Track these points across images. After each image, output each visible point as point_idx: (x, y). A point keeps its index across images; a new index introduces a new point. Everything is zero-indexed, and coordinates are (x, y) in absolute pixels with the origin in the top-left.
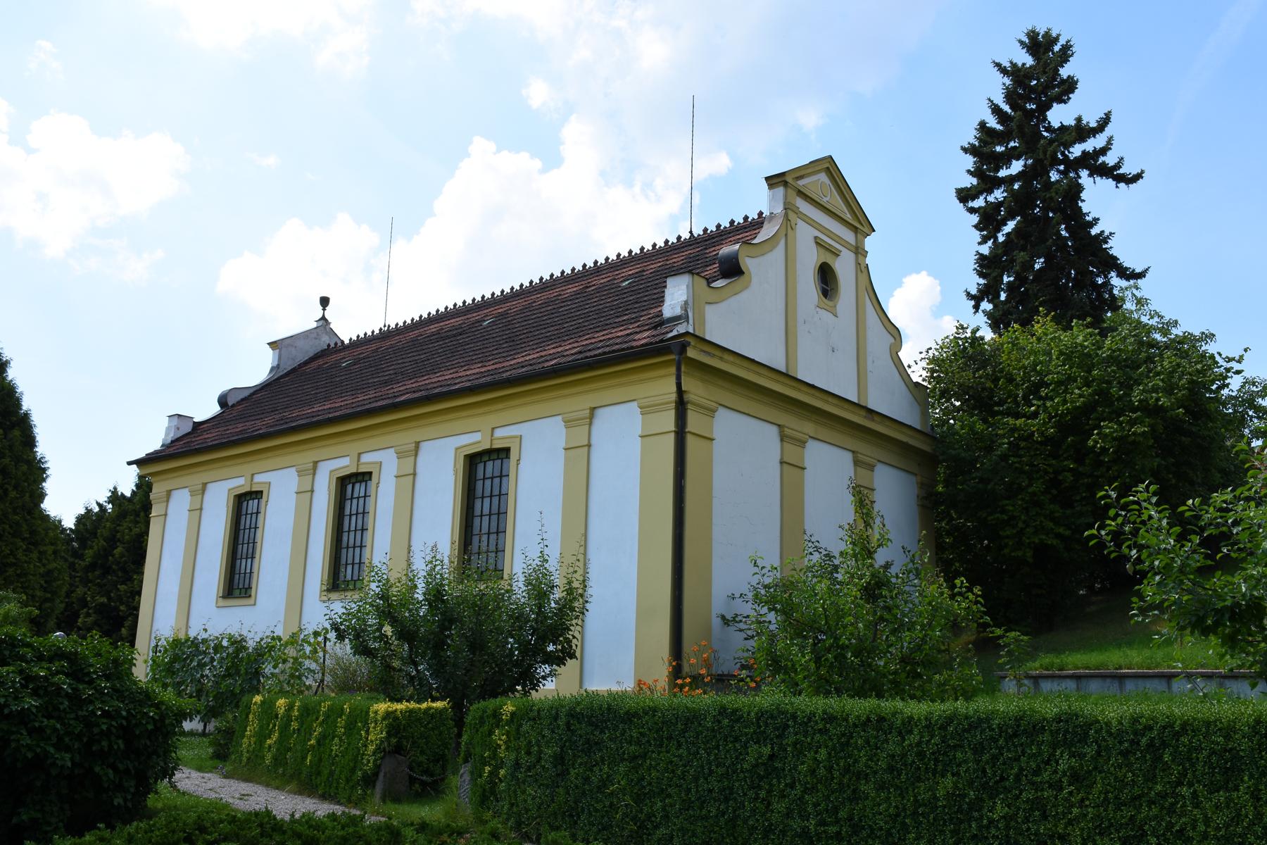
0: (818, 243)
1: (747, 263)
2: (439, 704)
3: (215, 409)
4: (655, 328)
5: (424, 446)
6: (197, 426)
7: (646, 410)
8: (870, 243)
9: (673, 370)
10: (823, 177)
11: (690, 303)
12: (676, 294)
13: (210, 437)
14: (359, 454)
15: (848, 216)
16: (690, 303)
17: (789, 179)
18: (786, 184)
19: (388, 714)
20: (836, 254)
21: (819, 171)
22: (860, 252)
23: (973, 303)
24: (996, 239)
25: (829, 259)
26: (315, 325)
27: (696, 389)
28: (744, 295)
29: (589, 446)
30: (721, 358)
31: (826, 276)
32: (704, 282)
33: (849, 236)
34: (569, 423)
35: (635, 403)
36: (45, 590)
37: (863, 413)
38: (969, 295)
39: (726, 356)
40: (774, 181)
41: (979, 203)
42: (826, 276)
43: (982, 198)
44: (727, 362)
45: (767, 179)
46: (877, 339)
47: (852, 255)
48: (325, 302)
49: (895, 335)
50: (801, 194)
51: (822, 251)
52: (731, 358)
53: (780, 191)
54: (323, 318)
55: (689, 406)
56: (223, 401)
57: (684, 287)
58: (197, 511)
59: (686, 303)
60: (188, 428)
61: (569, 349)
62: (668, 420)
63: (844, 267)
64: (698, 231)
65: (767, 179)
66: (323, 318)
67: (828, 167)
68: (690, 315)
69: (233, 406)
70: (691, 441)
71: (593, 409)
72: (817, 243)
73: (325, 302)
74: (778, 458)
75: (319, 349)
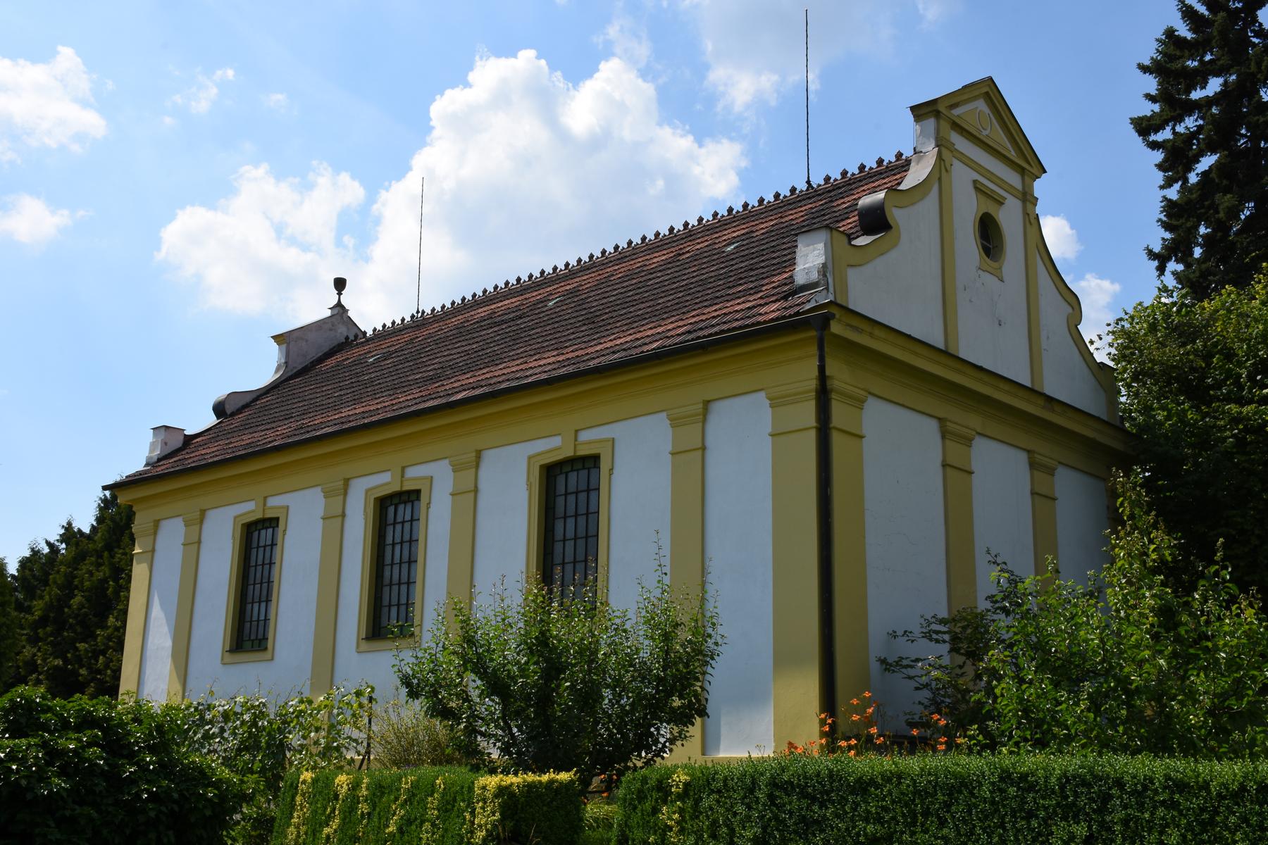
0: (978, 187)
1: (896, 215)
2: (564, 776)
3: (211, 420)
4: (785, 298)
5: (489, 456)
6: (189, 439)
7: (776, 402)
8: (1040, 187)
9: (814, 350)
10: (981, 105)
11: (830, 265)
12: (810, 257)
13: (210, 453)
14: (403, 469)
15: (1012, 154)
16: (830, 265)
17: (942, 108)
18: (937, 114)
19: (502, 791)
21: (975, 98)
22: (1028, 199)
23: (1156, 263)
24: (1186, 180)
26: (328, 313)
28: (893, 254)
29: (704, 448)
30: (871, 335)
31: (989, 233)
32: (845, 239)
33: (1014, 179)
34: (675, 422)
35: (763, 394)
37: (1041, 402)
38: (1151, 255)
39: (877, 332)
40: (920, 112)
41: (1165, 135)
42: (989, 233)
43: (1168, 129)
45: (913, 109)
47: (1018, 203)
48: (340, 284)
49: (1073, 302)
50: (957, 127)
51: (983, 199)
53: (931, 123)
54: (339, 305)
55: (833, 396)
56: (219, 409)
57: (821, 246)
58: (194, 545)
59: (824, 265)
60: (179, 442)
61: (673, 330)
62: (807, 413)
63: (1009, 218)
64: (817, 180)
65: (913, 109)
66: (339, 305)
67: (987, 91)
69: (233, 414)
70: (837, 440)
71: (707, 403)
72: (976, 188)
73: (340, 284)
75: (336, 343)
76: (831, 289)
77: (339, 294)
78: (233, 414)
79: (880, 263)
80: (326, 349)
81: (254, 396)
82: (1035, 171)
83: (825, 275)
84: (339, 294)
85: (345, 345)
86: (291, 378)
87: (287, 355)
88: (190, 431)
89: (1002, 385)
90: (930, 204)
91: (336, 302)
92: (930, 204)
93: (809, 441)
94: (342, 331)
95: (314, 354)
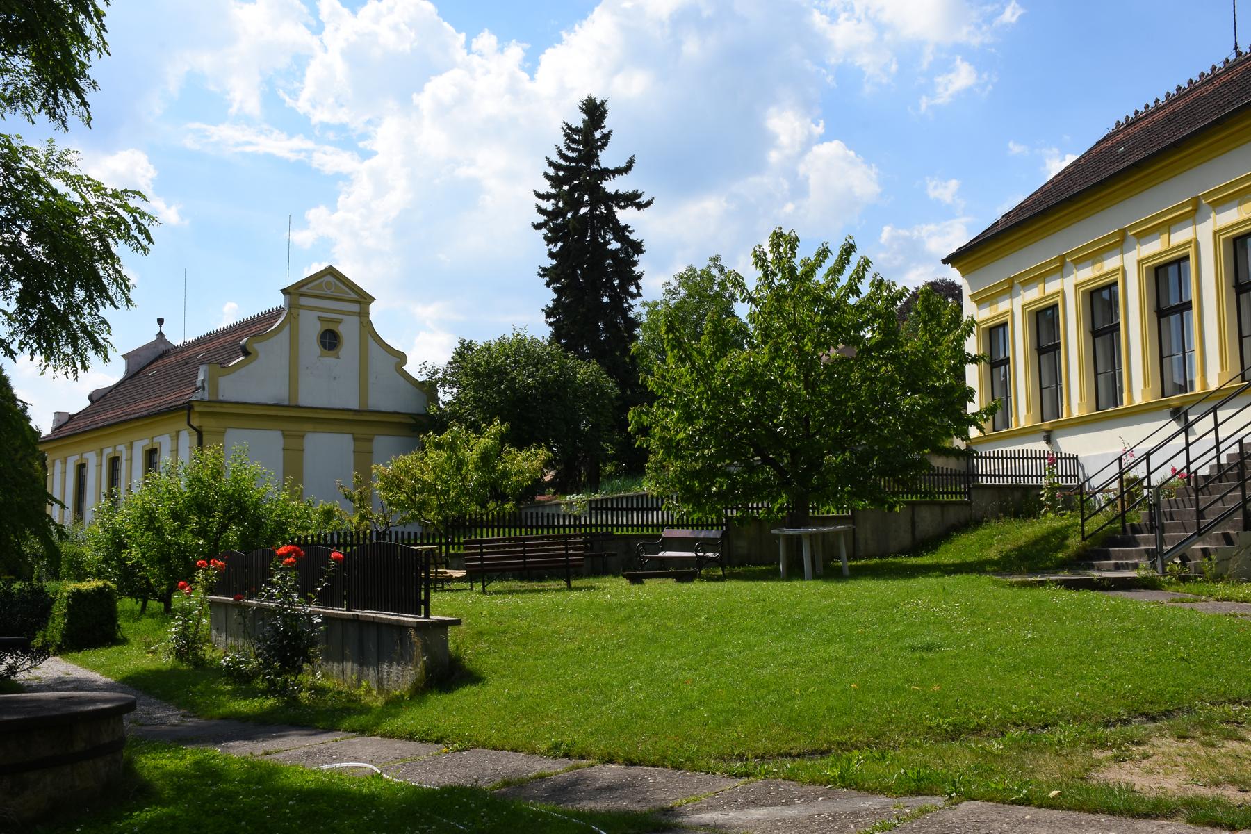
0: (321, 319)
1: (258, 347)
3: (89, 403)
6: (71, 417)
8: (372, 307)
10: (329, 278)
15: (354, 296)
17: (291, 291)
20: (340, 322)
22: (364, 314)
25: (332, 327)
27: (208, 424)
33: (355, 308)
40: (285, 291)
47: (356, 319)
48: (161, 321)
50: (302, 295)
56: (90, 398)
58: (64, 473)
59: (203, 381)
60: (66, 419)
67: (331, 271)
73: (161, 321)
79: (243, 371)
85: (163, 355)
86: (130, 378)
87: (128, 365)
88: (72, 412)
94: (162, 347)
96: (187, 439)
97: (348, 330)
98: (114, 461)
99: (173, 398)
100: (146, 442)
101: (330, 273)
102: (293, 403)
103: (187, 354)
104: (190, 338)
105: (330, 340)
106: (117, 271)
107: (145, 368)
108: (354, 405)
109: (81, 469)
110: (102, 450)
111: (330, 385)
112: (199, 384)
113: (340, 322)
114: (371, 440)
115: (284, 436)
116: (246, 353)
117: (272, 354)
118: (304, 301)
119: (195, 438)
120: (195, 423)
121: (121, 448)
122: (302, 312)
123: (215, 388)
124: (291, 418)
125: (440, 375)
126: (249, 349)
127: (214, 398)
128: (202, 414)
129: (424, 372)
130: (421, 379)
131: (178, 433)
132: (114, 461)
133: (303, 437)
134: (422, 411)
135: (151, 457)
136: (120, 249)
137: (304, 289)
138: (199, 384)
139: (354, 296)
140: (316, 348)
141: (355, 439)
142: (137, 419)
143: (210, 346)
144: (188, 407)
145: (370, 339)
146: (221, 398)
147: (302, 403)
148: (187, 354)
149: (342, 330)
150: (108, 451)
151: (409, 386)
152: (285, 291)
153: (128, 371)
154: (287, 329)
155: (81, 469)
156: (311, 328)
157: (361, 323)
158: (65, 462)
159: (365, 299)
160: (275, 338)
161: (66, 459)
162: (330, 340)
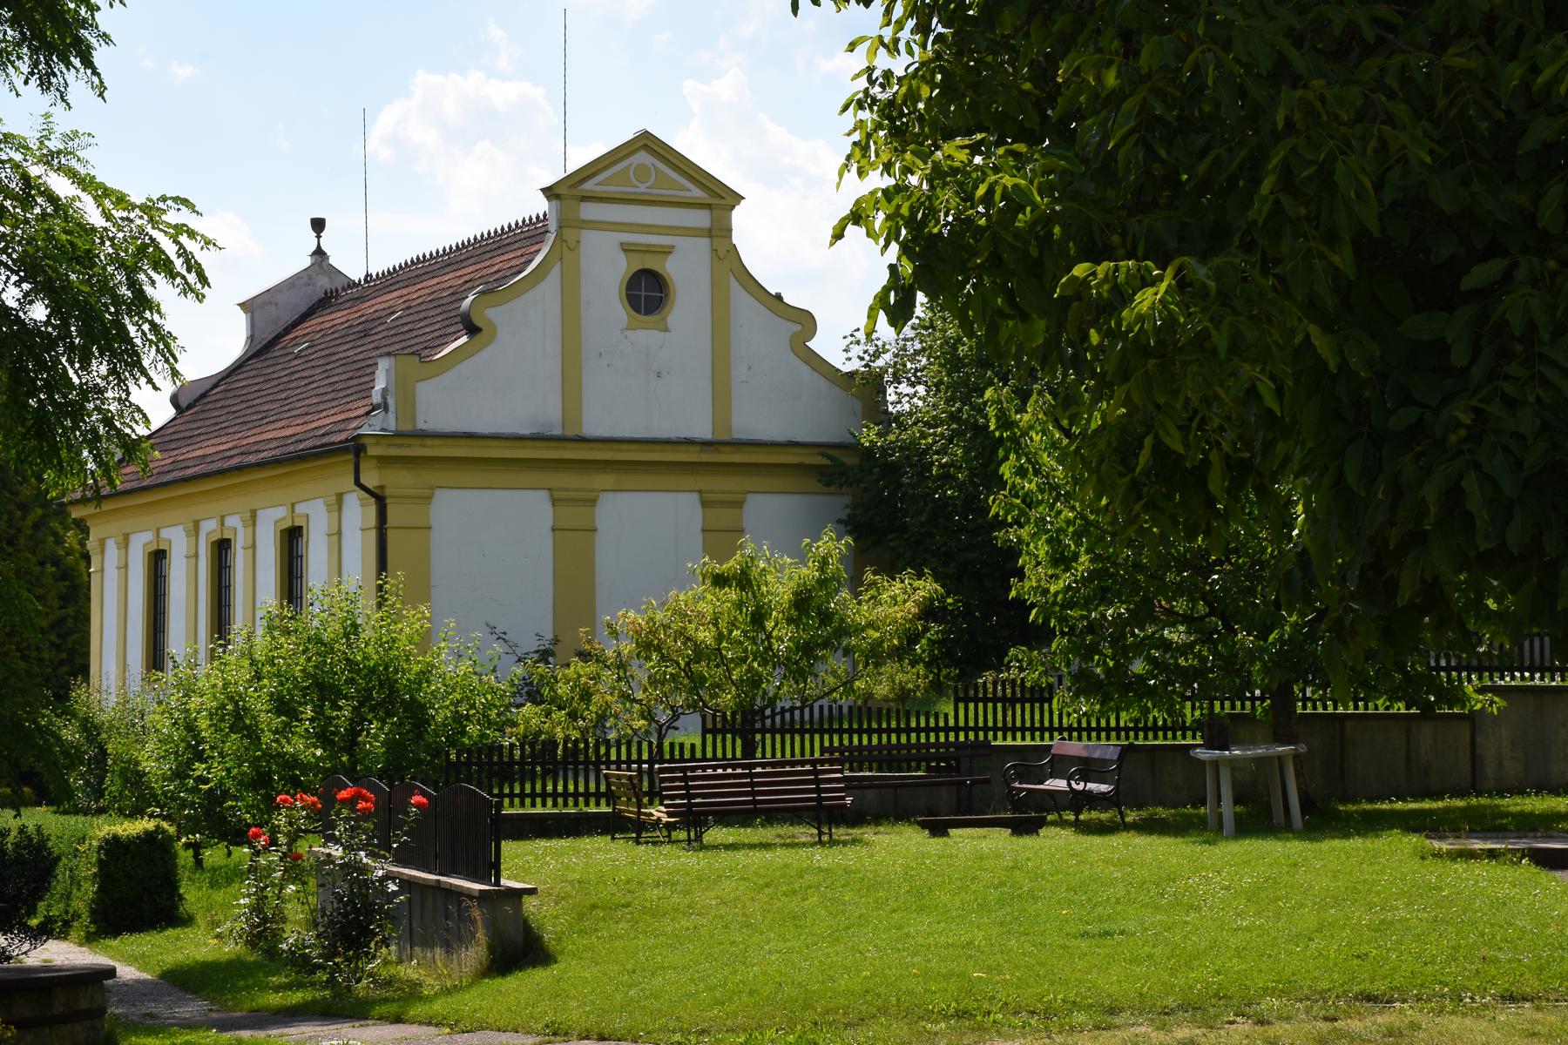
0: (627, 249)
1: (495, 315)
3: (171, 412)
5: (259, 513)
8: (738, 216)
10: (643, 158)
11: (392, 389)
16: (392, 389)
17: (561, 191)
18: (558, 197)
20: (667, 251)
21: (637, 150)
22: (720, 232)
25: (651, 263)
26: (307, 262)
27: (397, 481)
33: (700, 219)
36: (58, 648)
39: (429, 442)
40: (549, 192)
44: (432, 446)
46: (755, 336)
47: (704, 243)
48: (318, 225)
49: (805, 322)
50: (585, 199)
52: (438, 442)
54: (319, 253)
58: (124, 567)
59: (385, 391)
66: (319, 253)
67: (646, 143)
68: (391, 401)
69: (189, 407)
70: (391, 536)
73: (318, 225)
74: (550, 523)
75: (316, 299)
76: (392, 408)
77: (319, 237)
78: (189, 407)
80: (303, 309)
81: (207, 386)
82: (729, 201)
83: (384, 398)
84: (319, 237)
85: (326, 302)
87: (253, 325)
89: (624, 447)
90: (551, 287)
91: (314, 247)
92: (551, 287)
93: (373, 534)
94: (324, 283)
95: (288, 318)
96: (358, 513)
97: (686, 269)
98: (222, 548)
99: (326, 423)
100: (281, 512)
101: (646, 147)
102: (569, 433)
103: (370, 308)
104: (377, 268)
105: (647, 292)
106: (155, 327)
107: (288, 330)
108: (703, 431)
109: (158, 559)
110: (196, 524)
111: (652, 387)
112: (376, 398)
113: (667, 251)
114: (739, 504)
115: (555, 502)
116: (472, 330)
117: (525, 324)
118: (590, 211)
119: (372, 511)
120: (370, 479)
121: (233, 521)
122: (590, 238)
123: (409, 404)
124: (568, 461)
125: (887, 357)
126: (477, 322)
127: (407, 427)
128: (384, 461)
129: (856, 350)
130: (847, 368)
131: (340, 497)
132: (222, 548)
133: (593, 502)
134: (848, 439)
135: (292, 538)
136: (161, 290)
137: (589, 186)
138: (376, 398)
139: (696, 193)
140: (620, 312)
141: (705, 504)
142: (260, 465)
143: (417, 293)
144: (356, 448)
145: (735, 286)
146: (421, 425)
147: (591, 428)
148: (370, 308)
149: (671, 268)
150: (209, 527)
151: (823, 385)
152: (549, 192)
153: (251, 338)
154: (555, 274)
155: (158, 559)
156: (605, 266)
157: (714, 251)
158: (125, 544)
159: (721, 199)
160: (530, 295)
161: (126, 537)
162: (647, 292)
